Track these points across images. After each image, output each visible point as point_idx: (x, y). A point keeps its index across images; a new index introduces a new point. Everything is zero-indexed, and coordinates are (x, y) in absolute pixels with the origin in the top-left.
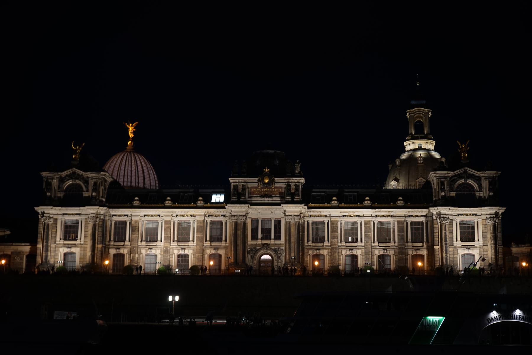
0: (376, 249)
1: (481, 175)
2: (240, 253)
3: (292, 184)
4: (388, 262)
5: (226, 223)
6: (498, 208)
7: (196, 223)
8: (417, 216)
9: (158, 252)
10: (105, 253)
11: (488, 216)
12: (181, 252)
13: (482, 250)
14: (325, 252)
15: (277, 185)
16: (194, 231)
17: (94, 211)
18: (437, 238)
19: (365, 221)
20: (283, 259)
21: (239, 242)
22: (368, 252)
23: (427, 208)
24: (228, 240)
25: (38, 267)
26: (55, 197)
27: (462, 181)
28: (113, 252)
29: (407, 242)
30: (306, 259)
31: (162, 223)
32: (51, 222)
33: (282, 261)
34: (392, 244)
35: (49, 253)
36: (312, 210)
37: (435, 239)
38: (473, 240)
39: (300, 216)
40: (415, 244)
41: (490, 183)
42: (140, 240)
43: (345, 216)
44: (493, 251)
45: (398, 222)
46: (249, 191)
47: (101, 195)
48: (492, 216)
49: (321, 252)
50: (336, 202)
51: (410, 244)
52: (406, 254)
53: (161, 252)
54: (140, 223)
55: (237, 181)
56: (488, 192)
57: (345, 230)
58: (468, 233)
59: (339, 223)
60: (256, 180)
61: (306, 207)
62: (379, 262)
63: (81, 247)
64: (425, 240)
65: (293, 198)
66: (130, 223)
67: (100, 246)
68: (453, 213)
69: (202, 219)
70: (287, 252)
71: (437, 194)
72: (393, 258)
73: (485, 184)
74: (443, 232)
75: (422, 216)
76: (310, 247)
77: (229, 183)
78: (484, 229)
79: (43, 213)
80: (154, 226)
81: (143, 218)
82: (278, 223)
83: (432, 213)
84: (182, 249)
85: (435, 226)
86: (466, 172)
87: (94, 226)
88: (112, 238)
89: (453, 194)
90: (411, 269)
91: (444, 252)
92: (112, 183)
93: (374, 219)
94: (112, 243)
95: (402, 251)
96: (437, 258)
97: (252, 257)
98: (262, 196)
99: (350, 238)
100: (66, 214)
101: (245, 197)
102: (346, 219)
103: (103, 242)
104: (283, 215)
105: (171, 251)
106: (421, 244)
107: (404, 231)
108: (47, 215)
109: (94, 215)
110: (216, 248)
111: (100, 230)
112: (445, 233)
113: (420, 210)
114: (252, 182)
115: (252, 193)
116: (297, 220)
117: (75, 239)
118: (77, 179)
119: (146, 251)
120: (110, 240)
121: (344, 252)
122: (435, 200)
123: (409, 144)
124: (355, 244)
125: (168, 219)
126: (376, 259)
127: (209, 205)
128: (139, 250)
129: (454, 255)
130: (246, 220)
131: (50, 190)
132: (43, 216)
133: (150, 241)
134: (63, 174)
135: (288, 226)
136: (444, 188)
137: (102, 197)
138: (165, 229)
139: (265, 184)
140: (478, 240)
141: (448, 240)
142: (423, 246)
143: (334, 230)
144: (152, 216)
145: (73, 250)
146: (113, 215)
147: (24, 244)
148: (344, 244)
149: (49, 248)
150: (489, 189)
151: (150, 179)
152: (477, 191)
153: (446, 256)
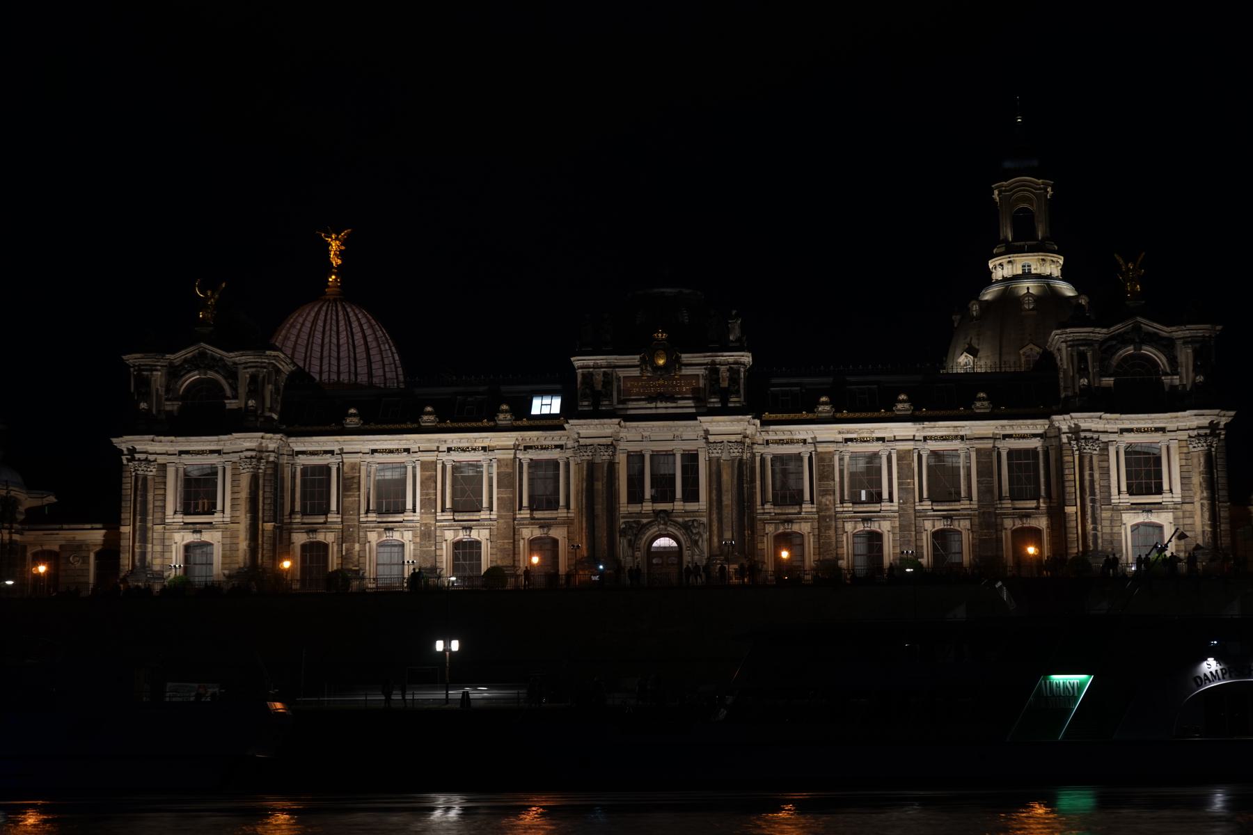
0: (926, 517)
1: (1175, 335)
2: (602, 534)
3: (723, 368)
4: (955, 548)
5: (567, 465)
6: (1216, 411)
7: (495, 465)
8: (1023, 437)
9: (408, 535)
10: (281, 542)
11: (1194, 433)
12: (462, 535)
13: (1180, 514)
14: (805, 528)
15: (685, 371)
16: (491, 486)
17: (253, 445)
18: (1072, 489)
19: (898, 452)
20: (706, 549)
21: (600, 508)
22: (908, 526)
23: (1047, 416)
24: (572, 505)
25: (124, 580)
26: (159, 411)
27: (1130, 350)
28: (299, 539)
29: (1001, 498)
30: (760, 546)
31: (414, 468)
32: (152, 471)
33: (702, 552)
34: (964, 504)
35: (150, 546)
36: (772, 427)
37: (1068, 489)
38: (1159, 491)
39: (742, 443)
41: (1197, 355)
42: (362, 511)
43: (851, 440)
44: (1207, 515)
45: (978, 451)
46: (619, 386)
47: (268, 404)
48: (1202, 432)
49: (796, 528)
50: (827, 408)
51: (1007, 504)
52: (999, 528)
53: (414, 536)
55: (591, 363)
56: (1191, 375)
57: (852, 474)
58: (1145, 474)
59: (836, 458)
60: (635, 359)
61: (758, 422)
62: (935, 548)
63: (225, 530)
64: (1043, 493)
65: (724, 401)
66: (338, 469)
67: (269, 526)
68: (1109, 427)
69: (509, 455)
70: (715, 528)
72: (966, 538)
73: (1185, 355)
74: (1087, 473)
75: (1035, 436)
76: (767, 517)
77: (572, 369)
78: (1184, 462)
79: (132, 451)
80: (397, 475)
81: (369, 458)
82: (691, 460)
83: (1059, 429)
84: (464, 528)
85: (1066, 459)
86: (1137, 328)
87: (255, 478)
88: (298, 508)
89: (1108, 381)
90: (1010, 562)
91: (1090, 521)
92: (292, 373)
93: (920, 445)
95: (987, 521)
96: (1072, 536)
97: (631, 545)
98: (651, 399)
99: (863, 492)
100: (187, 452)
101: (611, 400)
102: (853, 447)
103: (276, 516)
104: (702, 443)
105: (438, 533)
106: (1032, 504)
107: (991, 474)
108: (143, 456)
109: (253, 454)
110: (545, 525)
111: (267, 489)
113: (1029, 422)
114: (627, 365)
116: (736, 453)
117: (211, 511)
119: (380, 535)
120: (293, 512)
121: (849, 527)
122: (1066, 397)
123: (1001, 265)
124: (876, 507)
125: (429, 457)
126: (926, 541)
127: (525, 422)
128: (362, 534)
129: (1112, 527)
130: (614, 454)
131: (146, 396)
132: (133, 459)
133: (388, 512)
134: (177, 357)
135: (714, 468)
136: (1086, 368)
137: (271, 410)
140: (1171, 491)
141: (1097, 491)
142: (1037, 508)
143: (826, 475)
144: (391, 451)
145: (206, 536)
147: (89, 526)
148: (848, 506)
149: (150, 534)
150: (1195, 366)
151: (384, 365)
152: (1166, 374)
153: (1095, 529)
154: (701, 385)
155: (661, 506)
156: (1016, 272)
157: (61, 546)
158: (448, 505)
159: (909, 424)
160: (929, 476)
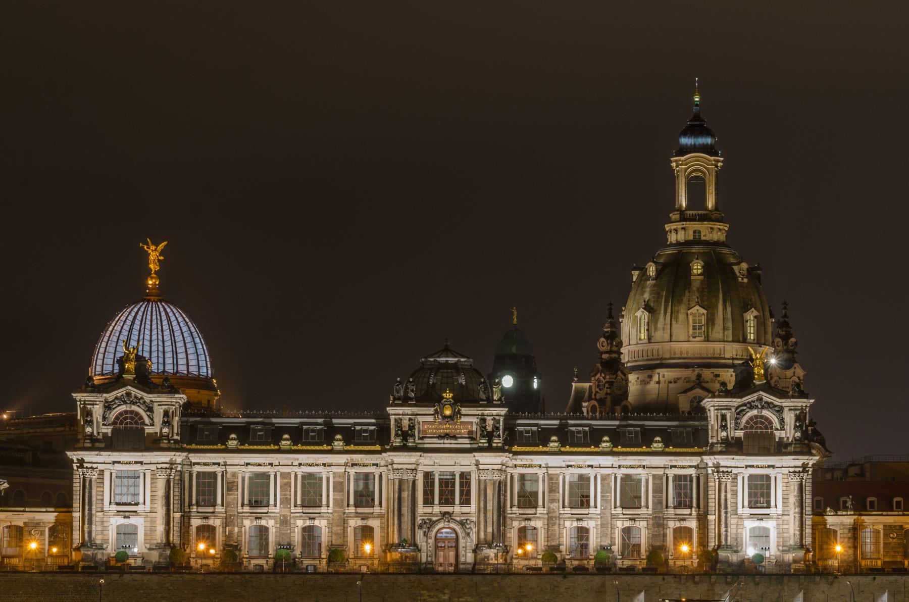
1: (784, 404)
2: (407, 525)
3: (489, 418)
5: (381, 476)
6: (807, 457)
8: (683, 467)
11: (792, 470)
13: (781, 522)
14: (538, 524)
15: (464, 419)
18: (713, 504)
19: (602, 475)
20: (474, 536)
21: (406, 510)
22: (606, 525)
25: (77, 549)
27: (755, 412)
29: (667, 507)
30: (508, 535)
33: (472, 540)
34: (643, 511)
35: (94, 527)
36: (519, 457)
37: (710, 504)
38: (769, 507)
40: (679, 511)
41: (798, 418)
43: (571, 466)
45: (654, 476)
46: (419, 428)
47: (175, 431)
48: (797, 470)
49: (533, 523)
51: (671, 511)
52: (664, 527)
54: (240, 476)
55: (401, 412)
56: (793, 431)
58: (760, 492)
60: (431, 410)
62: (623, 539)
65: (490, 441)
66: (223, 475)
67: (178, 515)
69: (341, 470)
70: (482, 526)
71: (715, 434)
73: (790, 418)
74: (723, 494)
75: (691, 467)
77: (387, 417)
78: (785, 488)
79: (81, 462)
81: (244, 469)
84: (310, 518)
85: (710, 484)
86: (760, 399)
88: (194, 502)
89: (740, 434)
93: (616, 471)
94: (194, 509)
96: (711, 535)
97: (425, 534)
98: (440, 437)
100: (119, 462)
102: (571, 470)
104: (474, 468)
105: (292, 521)
106: (687, 511)
107: (661, 492)
108: (89, 465)
109: (168, 466)
111: (176, 490)
112: (726, 496)
113: (688, 458)
115: (425, 432)
116: (497, 477)
118: (134, 404)
119: (252, 522)
121: (568, 524)
123: (676, 230)
125: (286, 470)
126: (618, 535)
129: (737, 529)
131: (90, 423)
132: (81, 466)
134: (110, 396)
135: (482, 486)
136: (726, 426)
138: (281, 487)
139: (445, 417)
141: (729, 506)
142: (690, 514)
143: (553, 489)
144: (260, 465)
146: (195, 464)
147: (44, 510)
149: (94, 519)
150: (796, 427)
152: (777, 430)
153: (726, 531)
154: (474, 429)
155: (445, 509)
156: (687, 239)
157: (25, 523)
158: (299, 502)
159: (610, 457)
160: (621, 499)
